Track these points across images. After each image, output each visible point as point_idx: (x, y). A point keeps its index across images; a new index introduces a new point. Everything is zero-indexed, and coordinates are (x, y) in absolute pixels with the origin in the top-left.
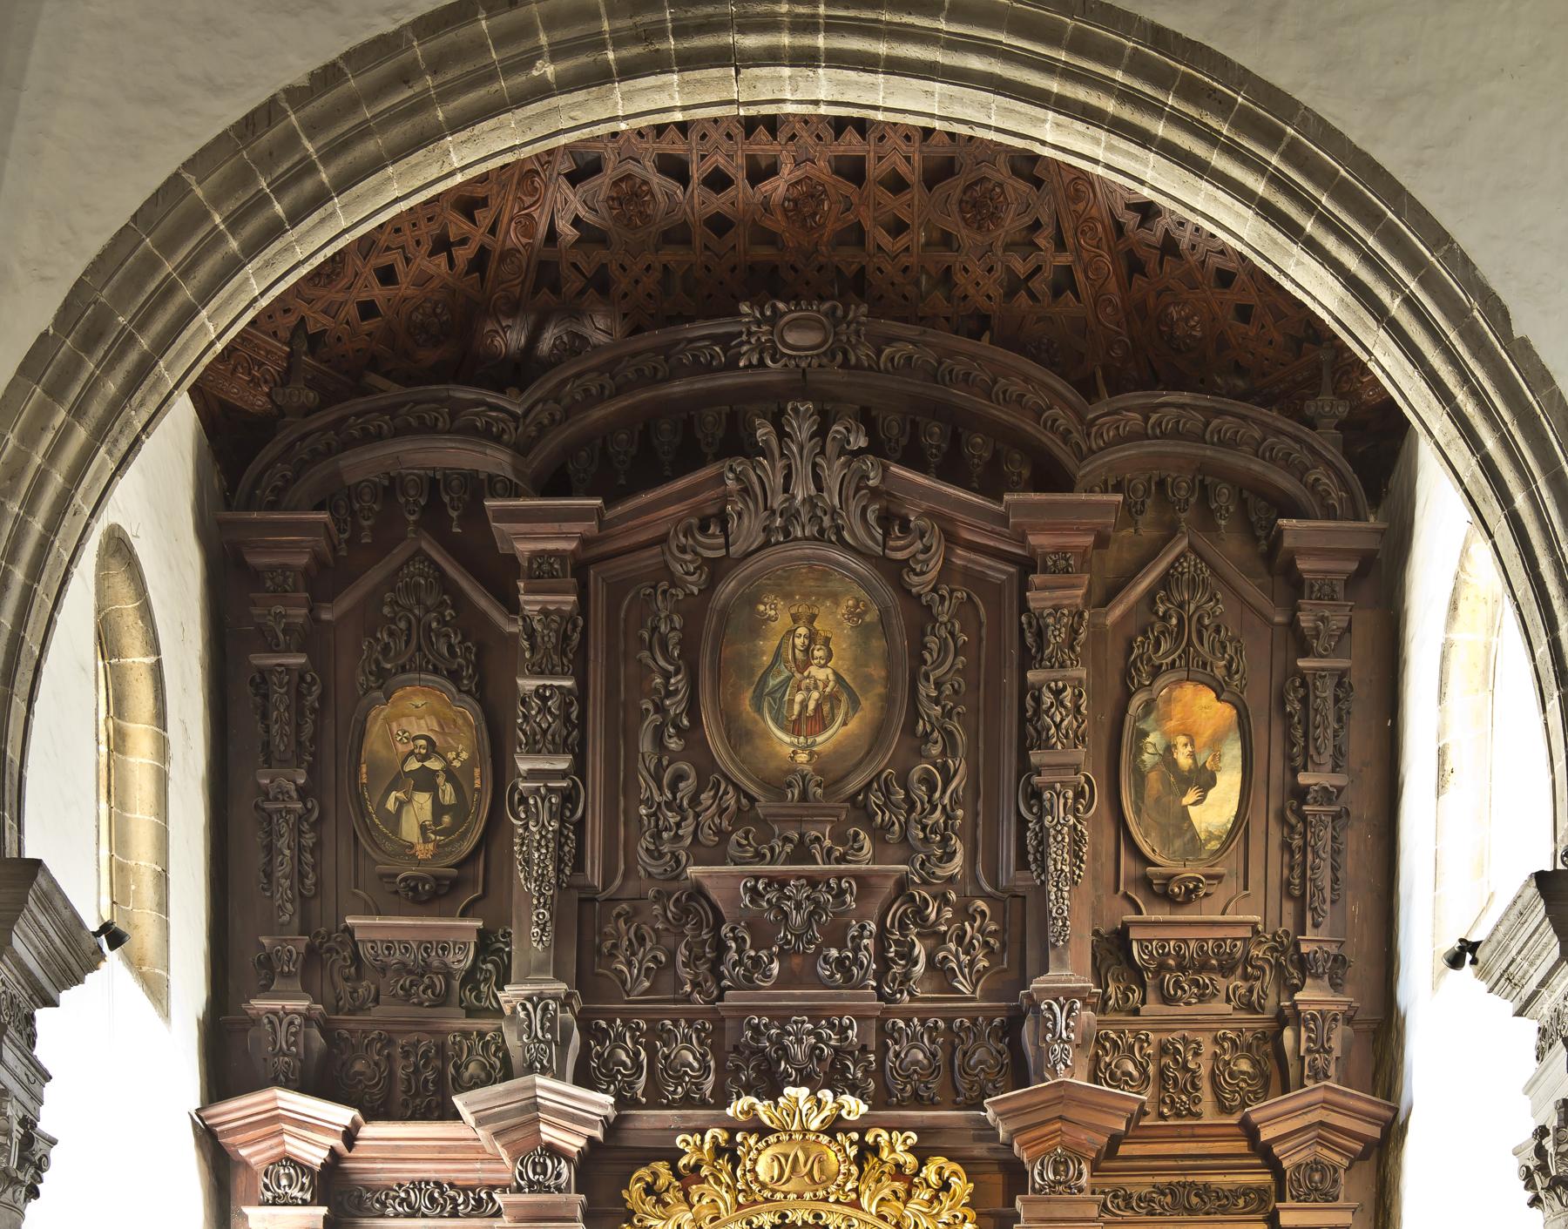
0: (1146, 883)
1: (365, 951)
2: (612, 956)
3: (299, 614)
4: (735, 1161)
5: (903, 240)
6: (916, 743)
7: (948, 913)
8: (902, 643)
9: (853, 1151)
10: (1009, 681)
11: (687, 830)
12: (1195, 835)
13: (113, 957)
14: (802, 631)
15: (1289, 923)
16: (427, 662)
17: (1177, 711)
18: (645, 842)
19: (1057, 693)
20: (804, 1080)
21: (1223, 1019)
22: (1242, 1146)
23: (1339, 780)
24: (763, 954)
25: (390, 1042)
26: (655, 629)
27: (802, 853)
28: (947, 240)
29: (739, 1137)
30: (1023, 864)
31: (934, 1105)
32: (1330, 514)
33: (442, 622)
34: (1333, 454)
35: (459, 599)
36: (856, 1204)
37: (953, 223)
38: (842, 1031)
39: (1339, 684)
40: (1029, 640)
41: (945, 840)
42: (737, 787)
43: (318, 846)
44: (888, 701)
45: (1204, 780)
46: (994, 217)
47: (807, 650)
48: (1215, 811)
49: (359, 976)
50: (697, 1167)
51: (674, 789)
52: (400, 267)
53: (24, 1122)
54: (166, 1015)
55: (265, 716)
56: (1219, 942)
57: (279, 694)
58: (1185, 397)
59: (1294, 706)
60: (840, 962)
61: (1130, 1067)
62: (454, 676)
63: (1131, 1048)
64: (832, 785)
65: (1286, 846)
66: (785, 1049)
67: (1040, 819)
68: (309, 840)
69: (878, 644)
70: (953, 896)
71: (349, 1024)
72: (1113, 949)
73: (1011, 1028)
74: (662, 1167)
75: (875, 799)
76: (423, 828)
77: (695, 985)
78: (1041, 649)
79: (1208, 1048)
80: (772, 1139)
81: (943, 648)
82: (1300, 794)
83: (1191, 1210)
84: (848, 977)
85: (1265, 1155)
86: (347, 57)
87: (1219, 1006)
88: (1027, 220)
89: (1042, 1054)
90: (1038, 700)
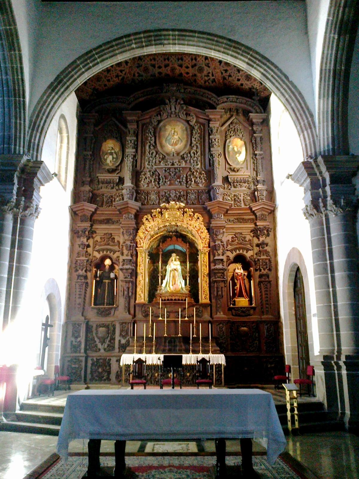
0: (230, 169)
1: (100, 180)
2: (141, 181)
3: (92, 129)
4: (162, 214)
5: (188, 76)
7: (198, 174)
8: (189, 132)
9: (182, 212)
10: (207, 138)
11: (154, 161)
12: (238, 161)
13: (55, 179)
14: (173, 130)
15: (255, 175)
16: (111, 137)
17: (234, 143)
18: (147, 163)
19: (215, 139)
20: (174, 200)
21: (245, 190)
22: (249, 211)
23: (262, 152)
24: (167, 180)
25: (103, 195)
26: (149, 131)
28: (195, 75)
29: (163, 210)
30: (210, 166)
31: (196, 205)
32: (257, 113)
33: (115, 130)
34: (258, 104)
35: (118, 127)
36: (183, 221)
37: (196, 73)
38: (180, 192)
39: (261, 138)
40: (210, 131)
41: (197, 162)
42: (162, 154)
43: (93, 164)
44: (187, 141)
46: (203, 72)
47: (174, 134)
48: (241, 157)
49: (99, 184)
50: (155, 216)
51: (152, 154)
52: (111, 79)
53: (36, 205)
54: (65, 190)
55: (85, 144)
56: (243, 178)
57: (88, 141)
58: (234, 96)
59: (253, 141)
60: (180, 182)
61: (229, 198)
62: (116, 138)
63: (229, 195)
64: (178, 154)
65: (254, 163)
66: (170, 196)
67: (213, 159)
68: (92, 163)
69: (185, 132)
70: (198, 171)
71: (95, 192)
72: (226, 179)
73: (209, 192)
74: (149, 215)
75: (185, 156)
76: (111, 161)
77: (155, 185)
78: (212, 133)
79: (242, 195)
80: (168, 210)
81: (196, 133)
82: (256, 155)
83: (241, 222)
84: (181, 184)
85: (253, 213)
86: (102, 44)
87: (244, 188)
88: (208, 72)
90: (212, 140)
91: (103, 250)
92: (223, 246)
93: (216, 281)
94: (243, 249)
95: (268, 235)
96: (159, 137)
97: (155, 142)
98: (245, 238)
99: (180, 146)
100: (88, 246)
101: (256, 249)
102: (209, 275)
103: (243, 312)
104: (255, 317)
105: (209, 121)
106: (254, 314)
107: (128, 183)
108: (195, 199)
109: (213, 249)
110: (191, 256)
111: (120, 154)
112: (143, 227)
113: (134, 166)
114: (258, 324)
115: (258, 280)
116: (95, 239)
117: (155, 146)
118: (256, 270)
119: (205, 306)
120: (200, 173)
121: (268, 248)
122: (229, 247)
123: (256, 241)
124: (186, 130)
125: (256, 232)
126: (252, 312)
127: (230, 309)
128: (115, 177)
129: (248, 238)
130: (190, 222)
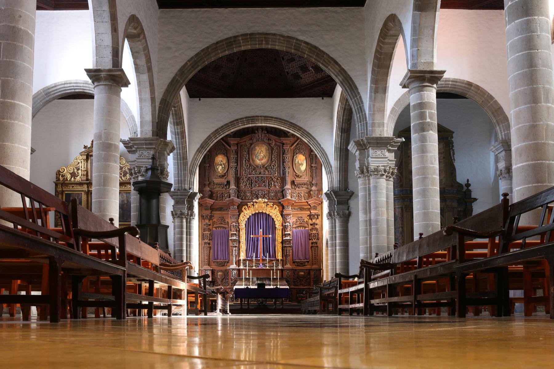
6: (272, 162)
8: (270, 151)
20: (261, 197)
27: (260, 173)
44: (269, 157)
45: (302, 164)
48: (303, 168)
64: (263, 166)
72: (293, 183)
89: (286, 195)
95: (318, 218)
97: (249, 158)
99: (264, 161)
100: (210, 225)
101: (310, 227)
102: (282, 243)
103: (301, 264)
104: (308, 267)
105: (283, 144)
106: (308, 265)
107: (233, 186)
108: (274, 196)
109: (284, 228)
111: (227, 164)
112: (242, 213)
113: (236, 174)
115: (311, 245)
117: (249, 161)
120: (277, 179)
121: (316, 226)
122: (294, 226)
123: (310, 222)
124: (269, 150)
125: (311, 216)
126: (306, 264)
128: (224, 181)
129: (306, 220)
130: (271, 211)
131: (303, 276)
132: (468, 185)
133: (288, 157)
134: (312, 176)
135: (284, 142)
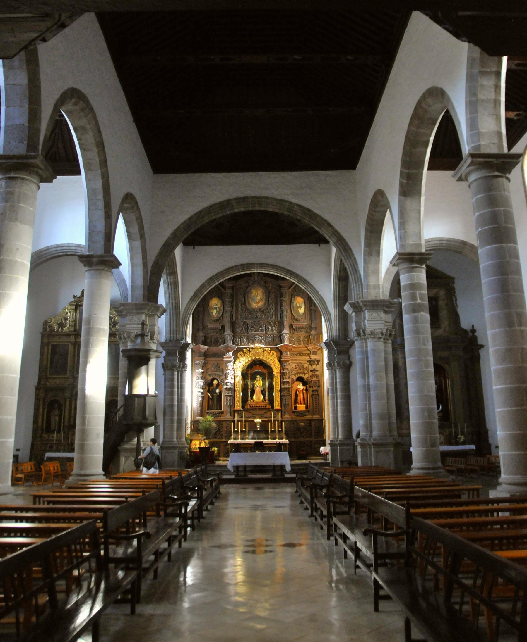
6: (269, 305)
10: (279, 299)
27: (257, 317)
44: (266, 301)
48: (302, 310)
72: (291, 326)
79: (302, 337)
87: (303, 333)
89: (284, 340)
91: (212, 375)
92: (289, 372)
93: (284, 395)
94: (302, 373)
95: (318, 364)
96: (248, 298)
98: (303, 366)
99: (261, 304)
101: (311, 373)
102: (281, 391)
103: (302, 414)
104: (309, 417)
105: (280, 287)
108: (271, 341)
109: (283, 375)
110: (268, 374)
111: (222, 308)
113: (232, 318)
114: (310, 421)
116: (207, 367)
118: (310, 387)
119: (278, 411)
120: (275, 323)
121: (317, 373)
122: (294, 372)
123: (310, 368)
125: (311, 362)
126: (307, 413)
127: (294, 412)
131: (304, 428)
132: (473, 331)
133: (286, 301)
134: (311, 319)
135: (281, 285)
